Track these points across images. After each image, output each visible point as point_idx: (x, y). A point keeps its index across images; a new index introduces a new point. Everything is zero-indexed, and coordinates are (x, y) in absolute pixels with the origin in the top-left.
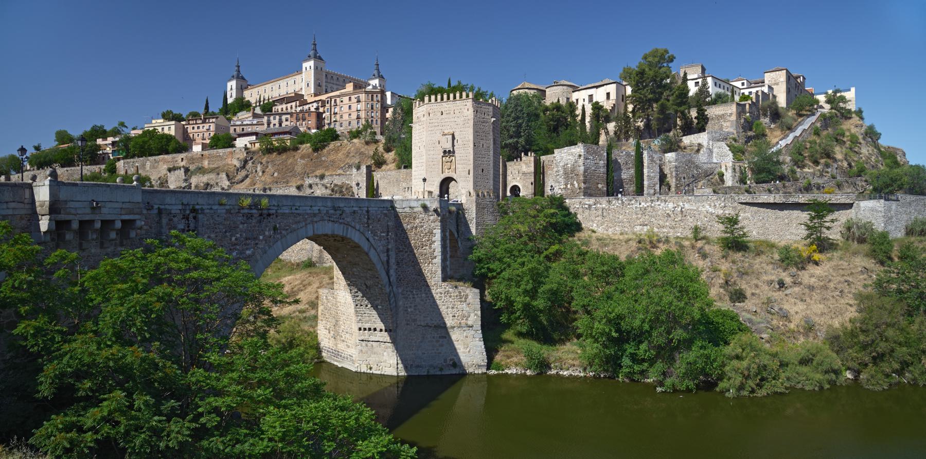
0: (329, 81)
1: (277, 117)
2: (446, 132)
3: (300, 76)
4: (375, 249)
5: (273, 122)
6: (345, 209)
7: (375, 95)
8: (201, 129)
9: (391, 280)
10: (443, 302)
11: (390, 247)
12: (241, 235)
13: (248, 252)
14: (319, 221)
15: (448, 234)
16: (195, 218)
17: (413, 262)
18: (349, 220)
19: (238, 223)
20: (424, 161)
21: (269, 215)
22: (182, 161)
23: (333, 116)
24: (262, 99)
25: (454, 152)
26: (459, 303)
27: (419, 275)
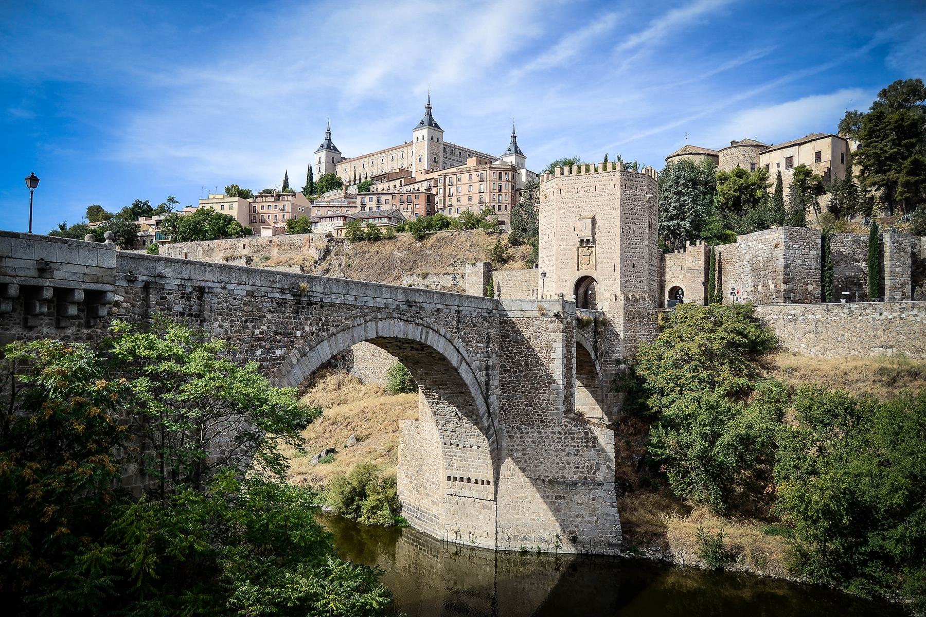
0: (448, 156)
1: (375, 198)
2: (584, 214)
3: (409, 148)
4: (467, 363)
5: (369, 204)
6: (424, 305)
7: (503, 173)
8: (272, 209)
9: (491, 409)
10: (562, 446)
11: (490, 363)
12: (268, 327)
13: (279, 352)
14: (385, 319)
15: (574, 350)
16: (200, 298)
17: (523, 386)
18: (429, 320)
19: (265, 310)
20: (554, 253)
21: (311, 304)
22: (244, 248)
23: (447, 199)
24: (358, 177)
25: (594, 241)
26: (586, 449)
27: (531, 406)
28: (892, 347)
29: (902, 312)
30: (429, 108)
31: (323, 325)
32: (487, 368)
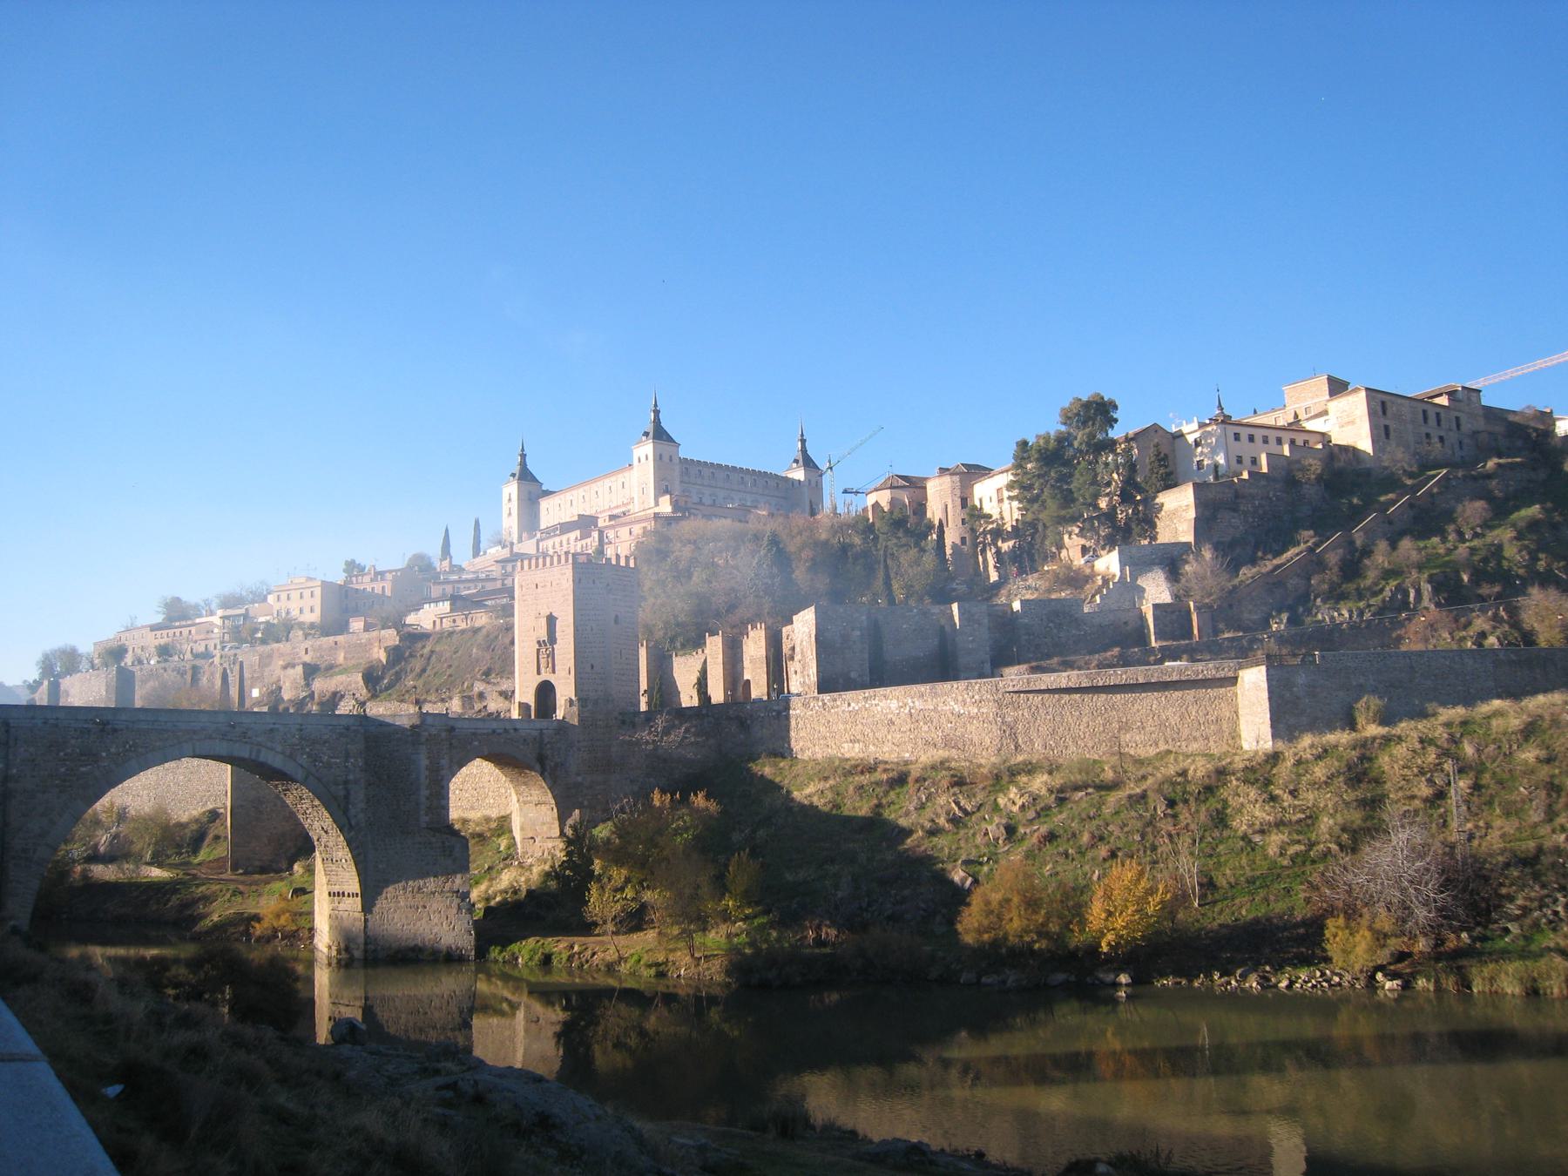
9: (353, 823)
11: (351, 777)
13: (83, 769)
18: (259, 739)
28: (858, 741)
29: (866, 702)
30: (523, 456)
31: (130, 747)
32: (346, 782)
